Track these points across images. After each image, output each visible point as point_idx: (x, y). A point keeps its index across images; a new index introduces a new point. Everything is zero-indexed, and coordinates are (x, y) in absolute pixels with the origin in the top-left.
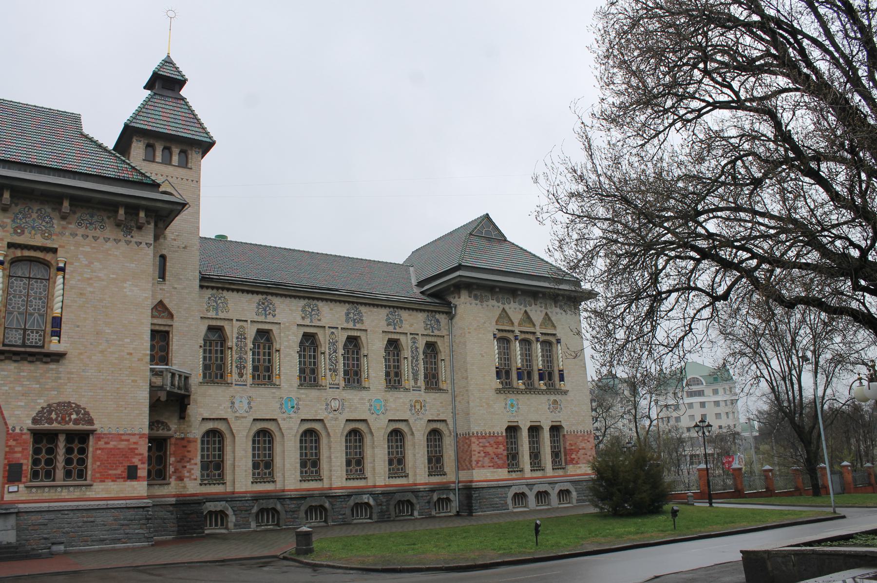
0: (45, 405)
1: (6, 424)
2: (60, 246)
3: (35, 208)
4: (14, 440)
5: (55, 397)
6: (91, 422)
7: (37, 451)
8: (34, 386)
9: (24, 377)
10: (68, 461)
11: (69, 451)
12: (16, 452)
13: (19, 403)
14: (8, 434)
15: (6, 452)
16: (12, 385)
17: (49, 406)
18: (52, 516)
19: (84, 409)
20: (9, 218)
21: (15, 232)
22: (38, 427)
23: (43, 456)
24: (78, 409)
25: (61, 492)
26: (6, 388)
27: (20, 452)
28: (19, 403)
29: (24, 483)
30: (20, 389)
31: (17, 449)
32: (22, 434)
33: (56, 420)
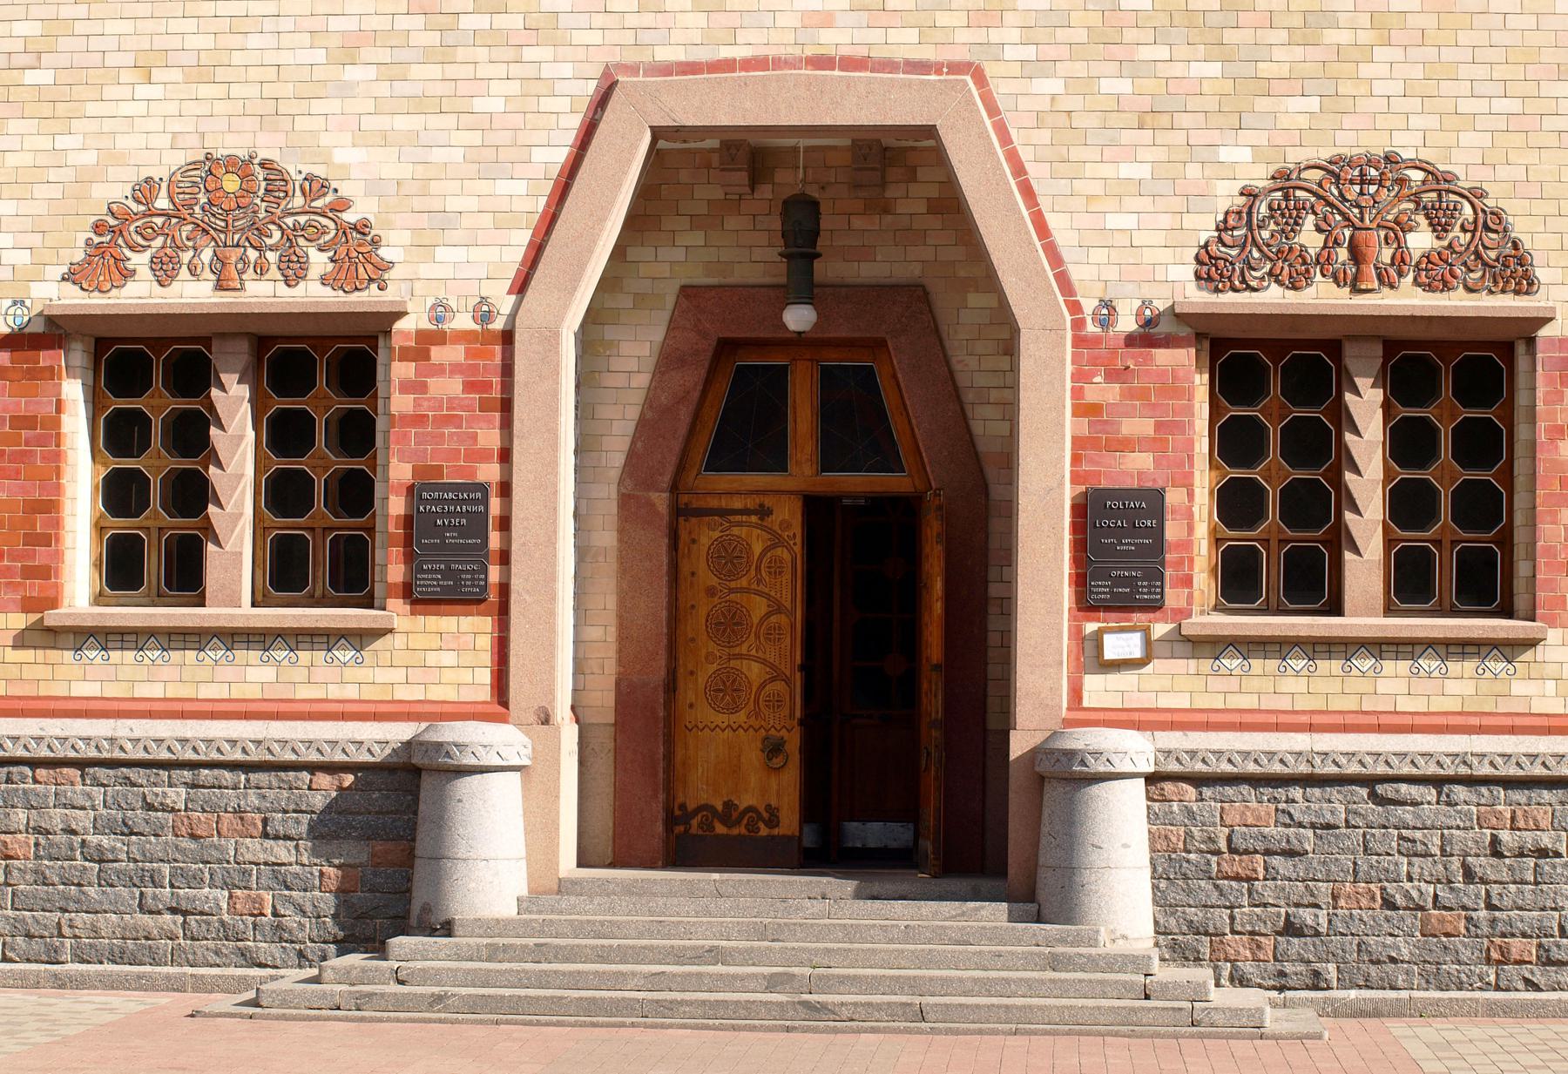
0: (1259, 177)
1: (1064, 281)
4: (1111, 376)
5: (1306, 132)
6: (1514, 271)
7: (1235, 442)
8: (1198, 69)
10: (1407, 505)
11: (1407, 443)
12: (1127, 445)
13: (1126, 170)
14: (1079, 341)
16: (1079, 69)
17: (1285, 181)
18: (1334, 804)
19: (1475, 195)
22: (1232, 301)
23: (1272, 473)
24: (1439, 197)
25: (1377, 674)
26: (1054, 86)
28: (1126, 170)
30: (1125, 86)
33: (1324, 261)
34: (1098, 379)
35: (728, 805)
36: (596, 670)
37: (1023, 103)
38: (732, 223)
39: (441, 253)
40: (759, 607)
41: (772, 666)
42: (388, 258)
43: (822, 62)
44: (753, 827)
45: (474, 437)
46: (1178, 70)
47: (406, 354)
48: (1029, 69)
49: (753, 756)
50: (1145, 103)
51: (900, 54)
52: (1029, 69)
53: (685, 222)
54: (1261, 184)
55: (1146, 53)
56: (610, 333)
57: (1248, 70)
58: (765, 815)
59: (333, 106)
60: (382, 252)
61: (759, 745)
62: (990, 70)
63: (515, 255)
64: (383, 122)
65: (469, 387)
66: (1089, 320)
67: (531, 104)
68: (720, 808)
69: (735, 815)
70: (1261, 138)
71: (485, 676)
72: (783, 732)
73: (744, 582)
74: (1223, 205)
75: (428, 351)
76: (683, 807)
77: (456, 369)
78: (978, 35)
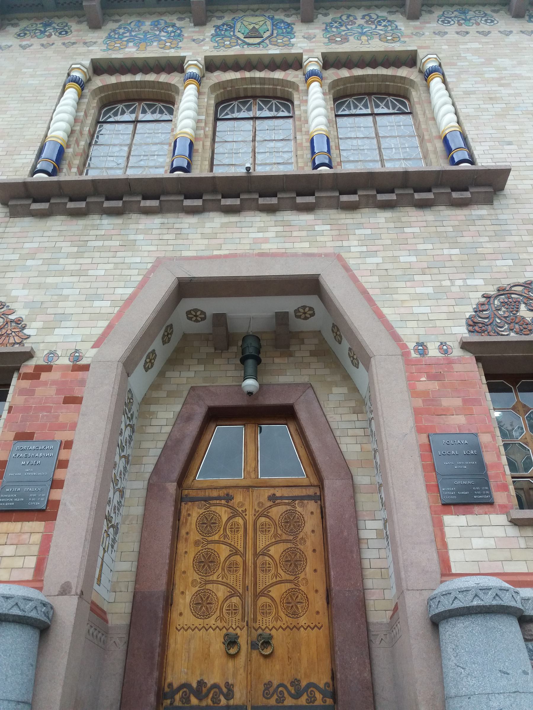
0: (492, 290)
1: (396, 338)
2: (421, 47)
3: (359, 14)
4: (431, 377)
8: (446, 252)
9: (414, 236)
12: (446, 412)
15: (417, 412)
16: (390, 254)
20: (316, 28)
21: (331, 40)
26: (379, 260)
27: (458, 411)
29: (504, 509)
31: (446, 402)
32: (450, 362)
34: (423, 379)
35: (201, 683)
36: (123, 589)
37: (362, 267)
38: (217, 361)
39: (57, 331)
40: (224, 552)
41: (232, 587)
42: (28, 334)
43: (262, 255)
44: (215, 700)
45: (57, 417)
46: (439, 252)
47: (26, 377)
48: (363, 255)
49: (217, 645)
50: (425, 265)
51: (300, 251)
52: (363, 255)
53: (196, 361)
54: (492, 293)
55: (421, 247)
56: (153, 408)
57: (474, 251)
58: (225, 690)
59: (19, 274)
60: (26, 331)
61: (223, 640)
62: (344, 255)
63: (100, 331)
64: (42, 280)
65: (58, 392)
66: (412, 352)
67: (118, 272)
68: (195, 685)
69: (204, 690)
70: (487, 276)
71: (32, 562)
72: (238, 631)
73: (216, 537)
74: (474, 302)
75: (40, 375)
76: (170, 685)
77: (54, 383)
78: (339, 244)
